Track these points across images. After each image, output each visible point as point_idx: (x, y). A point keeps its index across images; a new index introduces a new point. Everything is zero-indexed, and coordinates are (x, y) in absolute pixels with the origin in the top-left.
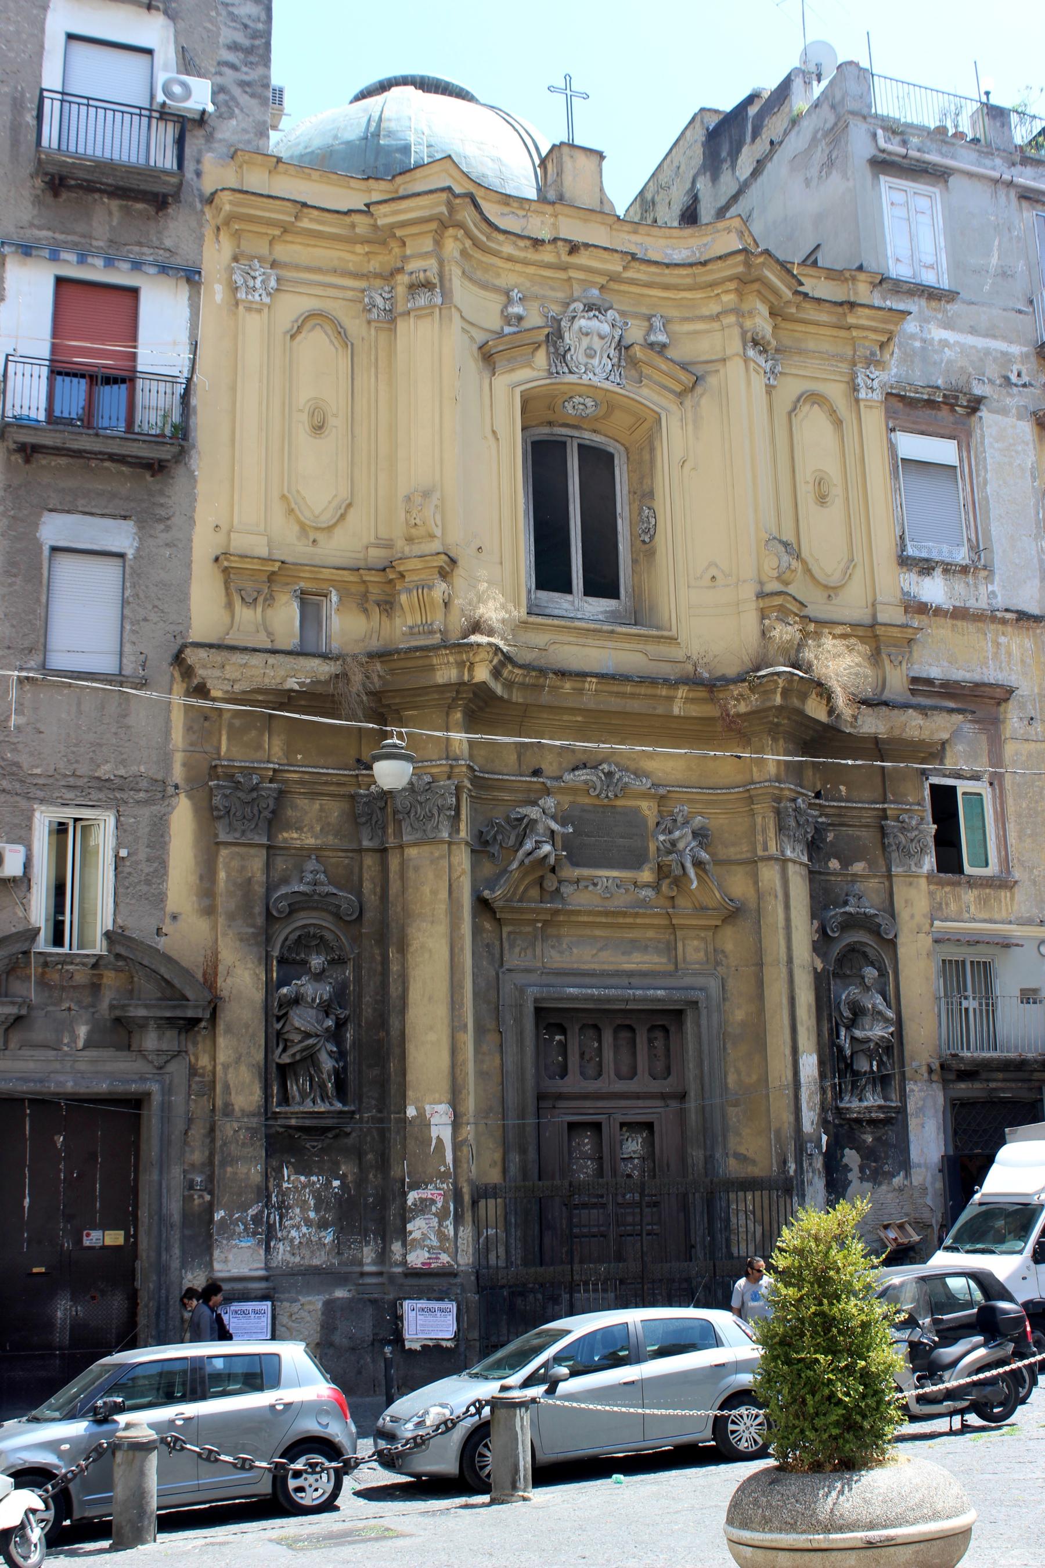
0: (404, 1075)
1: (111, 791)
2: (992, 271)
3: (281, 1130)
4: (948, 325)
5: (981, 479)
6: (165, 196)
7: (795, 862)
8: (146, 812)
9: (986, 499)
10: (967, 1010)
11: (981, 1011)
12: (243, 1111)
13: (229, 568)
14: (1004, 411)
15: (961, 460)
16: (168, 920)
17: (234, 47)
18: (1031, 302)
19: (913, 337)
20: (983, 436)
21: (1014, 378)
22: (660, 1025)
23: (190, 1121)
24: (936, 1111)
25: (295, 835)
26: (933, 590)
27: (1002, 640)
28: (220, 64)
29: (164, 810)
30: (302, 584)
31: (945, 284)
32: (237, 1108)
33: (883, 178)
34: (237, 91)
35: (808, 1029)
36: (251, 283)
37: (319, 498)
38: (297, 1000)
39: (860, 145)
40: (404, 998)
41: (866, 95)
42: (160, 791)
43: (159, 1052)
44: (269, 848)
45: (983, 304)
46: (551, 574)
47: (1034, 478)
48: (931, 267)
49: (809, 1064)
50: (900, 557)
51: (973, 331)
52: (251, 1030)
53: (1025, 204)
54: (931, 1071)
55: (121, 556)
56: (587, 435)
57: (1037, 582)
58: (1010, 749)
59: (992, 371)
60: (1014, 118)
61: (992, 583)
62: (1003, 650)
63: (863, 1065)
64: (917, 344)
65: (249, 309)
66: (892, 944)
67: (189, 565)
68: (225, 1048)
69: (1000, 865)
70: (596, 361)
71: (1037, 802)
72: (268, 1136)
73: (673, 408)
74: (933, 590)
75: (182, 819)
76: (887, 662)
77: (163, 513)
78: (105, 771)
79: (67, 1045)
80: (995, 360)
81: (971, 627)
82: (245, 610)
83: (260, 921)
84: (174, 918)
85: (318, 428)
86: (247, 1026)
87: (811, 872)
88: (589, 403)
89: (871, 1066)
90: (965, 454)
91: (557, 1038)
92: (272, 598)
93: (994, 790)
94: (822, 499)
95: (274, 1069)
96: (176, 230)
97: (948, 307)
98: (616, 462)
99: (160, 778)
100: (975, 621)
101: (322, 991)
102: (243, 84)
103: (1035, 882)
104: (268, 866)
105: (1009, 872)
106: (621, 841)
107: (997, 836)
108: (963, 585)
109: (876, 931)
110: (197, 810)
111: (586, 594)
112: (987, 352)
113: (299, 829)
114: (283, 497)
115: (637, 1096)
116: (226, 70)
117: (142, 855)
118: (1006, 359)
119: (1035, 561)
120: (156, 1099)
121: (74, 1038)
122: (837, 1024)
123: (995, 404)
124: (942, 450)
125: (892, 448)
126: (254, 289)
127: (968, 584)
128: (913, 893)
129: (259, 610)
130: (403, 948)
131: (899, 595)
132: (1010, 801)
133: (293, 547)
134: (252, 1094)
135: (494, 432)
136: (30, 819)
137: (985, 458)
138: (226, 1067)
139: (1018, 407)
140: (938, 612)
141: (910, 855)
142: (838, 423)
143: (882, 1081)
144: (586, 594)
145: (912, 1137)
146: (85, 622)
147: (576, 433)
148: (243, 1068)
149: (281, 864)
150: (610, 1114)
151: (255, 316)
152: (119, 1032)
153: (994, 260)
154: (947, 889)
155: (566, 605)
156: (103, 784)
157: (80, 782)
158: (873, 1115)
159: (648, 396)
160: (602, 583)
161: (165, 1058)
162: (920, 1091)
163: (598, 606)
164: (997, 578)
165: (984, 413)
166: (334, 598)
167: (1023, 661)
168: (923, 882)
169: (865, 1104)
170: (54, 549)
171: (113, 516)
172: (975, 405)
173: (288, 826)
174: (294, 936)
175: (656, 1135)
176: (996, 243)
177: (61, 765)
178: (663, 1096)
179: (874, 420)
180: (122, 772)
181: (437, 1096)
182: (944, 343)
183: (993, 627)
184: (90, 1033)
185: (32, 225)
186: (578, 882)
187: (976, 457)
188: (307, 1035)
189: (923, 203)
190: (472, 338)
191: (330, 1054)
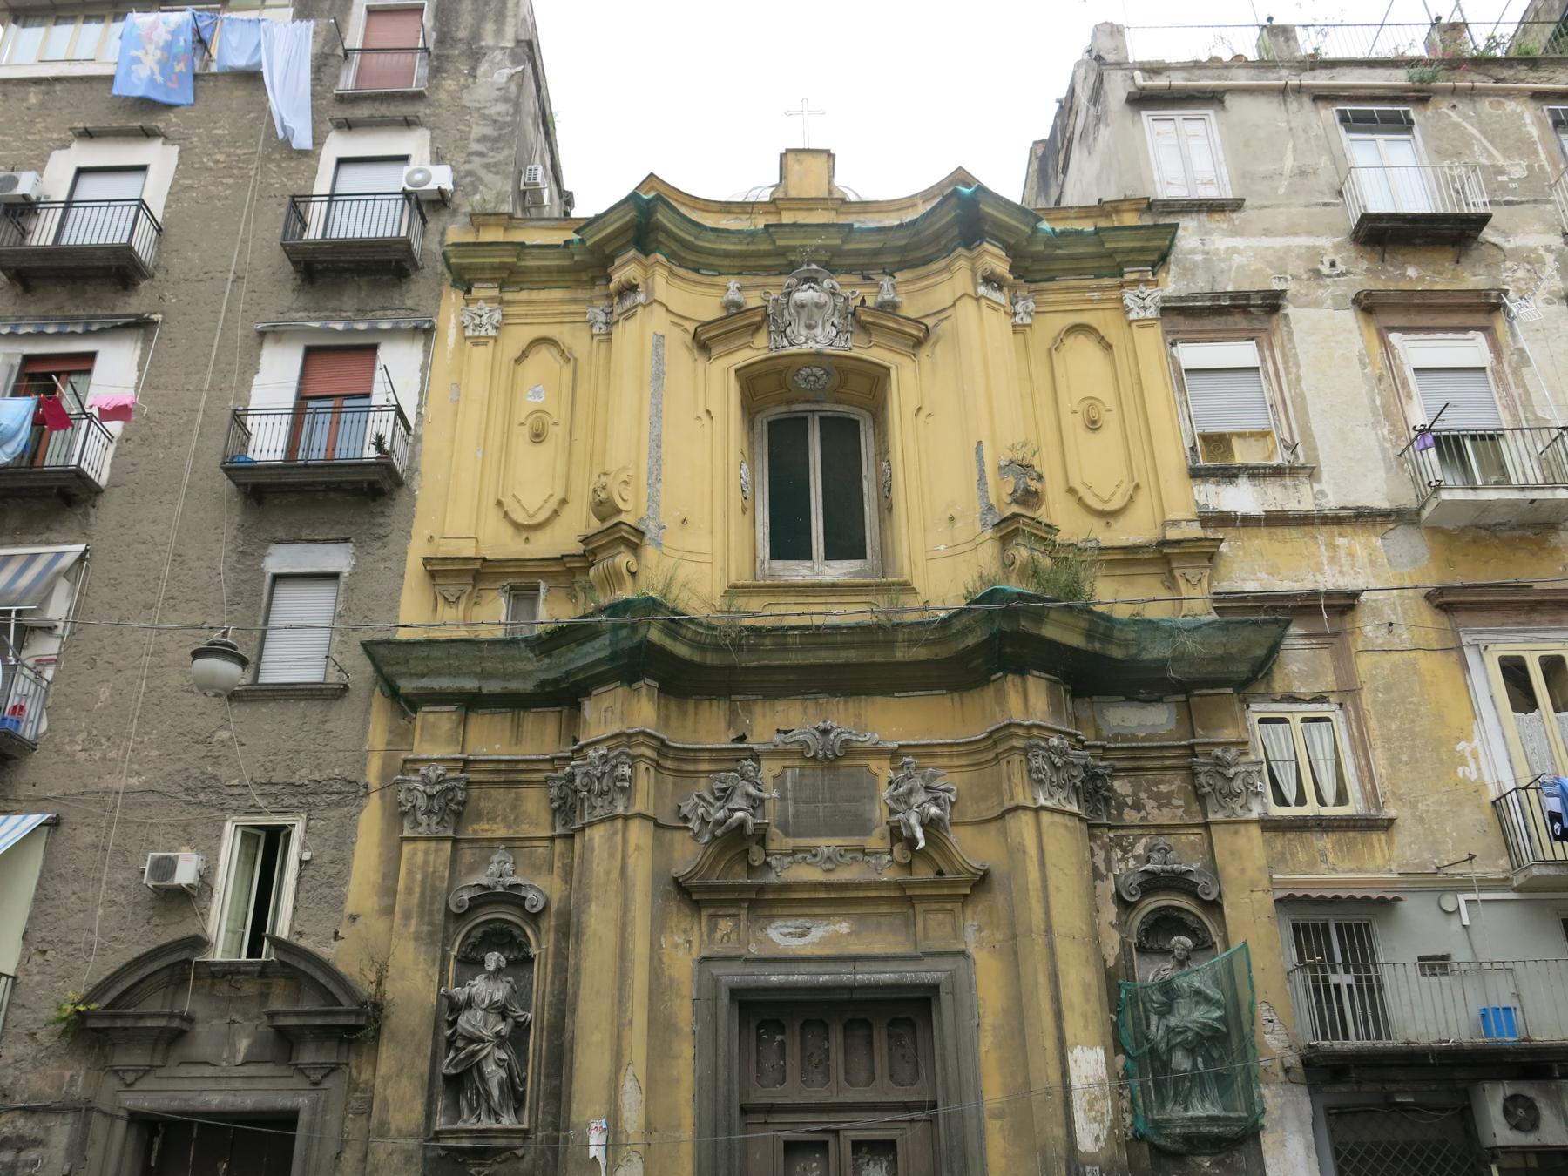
1: (304, 794)
2: (1287, 172)
3: (442, 1153)
4: (1236, 232)
5: (1293, 377)
6: (398, 262)
7: (1052, 810)
8: (334, 814)
9: (1302, 396)
10: (1337, 987)
11: (1360, 989)
12: (399, 1131)
13: (440, 571)
14: (1317, 304)
15: (1263, 360)
16: (345, 922)
17: (480, 140)
18: (1340, 193)
19: (1193, 252)
20: (1290, 333)
21: (1325, 269)
22: (903, 1016)
23: (343, 1144)
24: (1302, 1123)
25: (486, 827)
26: (1241, 498)
27: (1340, 541)
28: (469, 154)
29: (354, 811)
30: (510, 580)
31: (1228, 193)
32: (393, 1127)
33: (1144, 113)
34: (483, 173)
35: (1084, 1015)
36: (477, 320)
37: (532, 499)
38: (469, 1003)
39: (1117, 89)
40: (576, 994)
41: (1121, 48)
42: (354, 790)
43: (316, 1066)
44: (455, 841)
45: (1278, 206)
46: (788, 539)
47: (1364, 365)
48: (1211, 182)
49: (1089, 1063)
50: (1191, 469)
51: (1267, 232)
53: (1320, 104)
54: (1287, 1071)
55: (334, 576)
56: (827, 407)
57: (1382, 474)
58: (1364, 664)
59: (1296, 267)
60: (1299, 32)
61: (1319, 481)
62: (1342, 553)
63: (1181, 1061)
64: (1199, 257)
65: (476, 344)
66: (1215, 907)
67: (402, 576)
68: (388, 1055)
69: (1366, 800)
70: (819, 331)
71: (1413, 721)
72: (425, 1158)
73: (907, 361)
74: (1241, 498)
75: (371, 819)
76: (1182, 582)
77: (381, 531)
78: (301, 776)
79: (226, 1060)
80: (1299, 257)
81: (1294, 533)
82: (448, 609)
83: (439, 918)
84: (354, 918)
85: (538, 437)
86: (413, 1033)
87: (1090, 826)
88: (819, 372)
89: (1195, 1063)
90: (1267, 354)
91: (779, 1038)
92: (479, 596)
93: (1346, 712)
94: (1093, 425)
95: (440, 1081)
96: (415, 293)
97: (1235, 215)
98: (862, 427)
99: (351, 778)
100: (1299, 525)
101: (500, 992)
102: (487, 166)
103: (1421, 820)
104: (454, 860)
105: (1379, 809)
106: (846, 806)
107: (1358, 767)
108: (1278, 489)
109: (1189, 889)
110: (384, 808)
111: (827, 558)
112: (1288, 249)
113: (492, 820)
114: (499, 503)
115: (874, 1107)
116: (477, 159)
117: (326, 858)
118: (1315, 253)
119: (1377, 452)
120: (303, 1118)
121: (233, 1054)
122: (1146, 1011)
123: (1303, 299)
124: (1242, 353)
125: (1175, 362)
126: (481, 325)
127: (1285, 486)
128: (1241, 842)
129: (462, 607)
130: (579, 936)
131: (1194, 509)
132: (1373, 723)
133: (500, 543)
135: (708, 412)
136: (221, 828)
137: (1295, 355)
138: (386, 1080)
139: (1334, 298)
140: (1247, 521)
141: (1234, 795)
142: (1108, 347)
143: (1223, 1082)
144: (827, 558)
145: (1268, 1160)
146: (301, 643)
147: (816, 407)
148: (405, 1082)
149: (467, 856)
150: (837, 1132)
151: (481, 348)
152: (283, 1043)
153: (1289, 163)
154: (1290, 835)
155: (804, 572)
156: (295, 788)
157: (274, 790)
158: (1204, 1130)
159: (877, 355)
160: (846, 542)
161: (323, 1072)
162: (1274, 1096)
163: (839, 571)
164: (1325, 476)
165: (1290, 310)
166: (542, 589)
167: (1372, 563)
168: (1255, 831)
169: (1190, 1113)
170: (277, 578)
171: (336, 541)
172: (1272, 303)
173: (479, 817)
174: (478, 932)
175: (899, 1157)
176: (1290, 146)
177: (257, 775)
178: (907, 1107)
179: (1150, 340)
180: (316, 776)
182: (1234, 251)
183: (1323, 529)
184: (251, 1046)
185: (290, 309)
186: (794, 852)
187: (1284, 355)
188: (471, 1040)
189: (1196, 127)
190: (686, 330)
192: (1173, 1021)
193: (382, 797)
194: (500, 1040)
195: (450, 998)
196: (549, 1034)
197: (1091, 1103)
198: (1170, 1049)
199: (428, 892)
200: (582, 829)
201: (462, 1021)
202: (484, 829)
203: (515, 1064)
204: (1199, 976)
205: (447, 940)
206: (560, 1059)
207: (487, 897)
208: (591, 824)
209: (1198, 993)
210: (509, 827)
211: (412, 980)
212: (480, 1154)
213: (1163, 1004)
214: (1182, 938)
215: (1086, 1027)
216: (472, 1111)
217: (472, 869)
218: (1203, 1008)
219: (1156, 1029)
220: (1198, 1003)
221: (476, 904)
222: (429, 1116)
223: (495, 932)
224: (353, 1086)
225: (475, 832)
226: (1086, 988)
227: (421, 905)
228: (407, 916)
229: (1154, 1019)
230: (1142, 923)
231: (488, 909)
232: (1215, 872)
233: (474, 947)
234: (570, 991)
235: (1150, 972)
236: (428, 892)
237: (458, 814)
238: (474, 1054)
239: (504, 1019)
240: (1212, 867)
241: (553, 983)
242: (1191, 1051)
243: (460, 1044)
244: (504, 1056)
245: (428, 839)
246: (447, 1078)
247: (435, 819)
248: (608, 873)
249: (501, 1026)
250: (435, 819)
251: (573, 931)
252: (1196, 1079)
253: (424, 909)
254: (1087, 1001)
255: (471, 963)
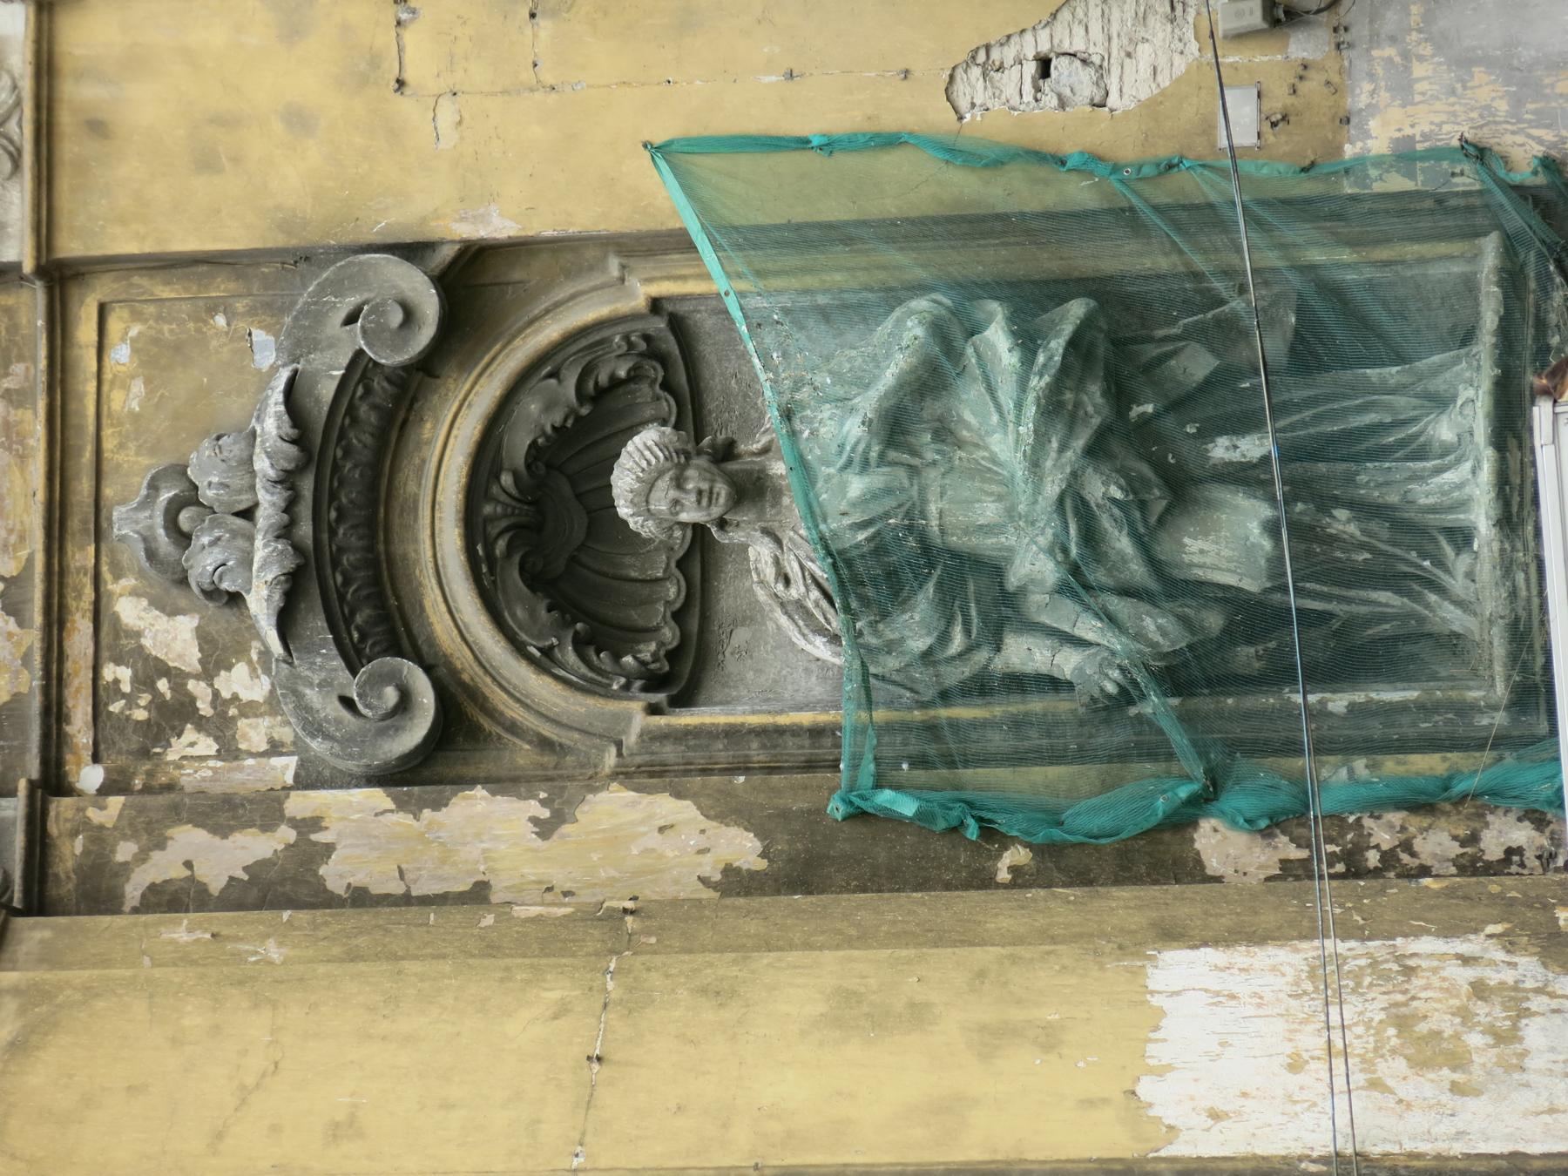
35: (992, 1040)
63: (1231, 543)
66: (475, 284)
122: (981, 687)
162: (1403, 89)
192: (1034, 565)
197: (1431, 1052)
198: (1172, 586)
204: (816, 396)
209: (894, 428)
213: (948, 604)
214: (624, 480)
215: (1049, 1039)
218: (969, 406)
219: (1074, 650)
220: (944, 432)
226: (852, 1015)
229: (1023, 653)
230: (545, 662)
232: (304, 258)
235: (790, 657)
240: (281, 271)
242: (1179, 489)
252: (1309, 479)
254: (919, 1015)
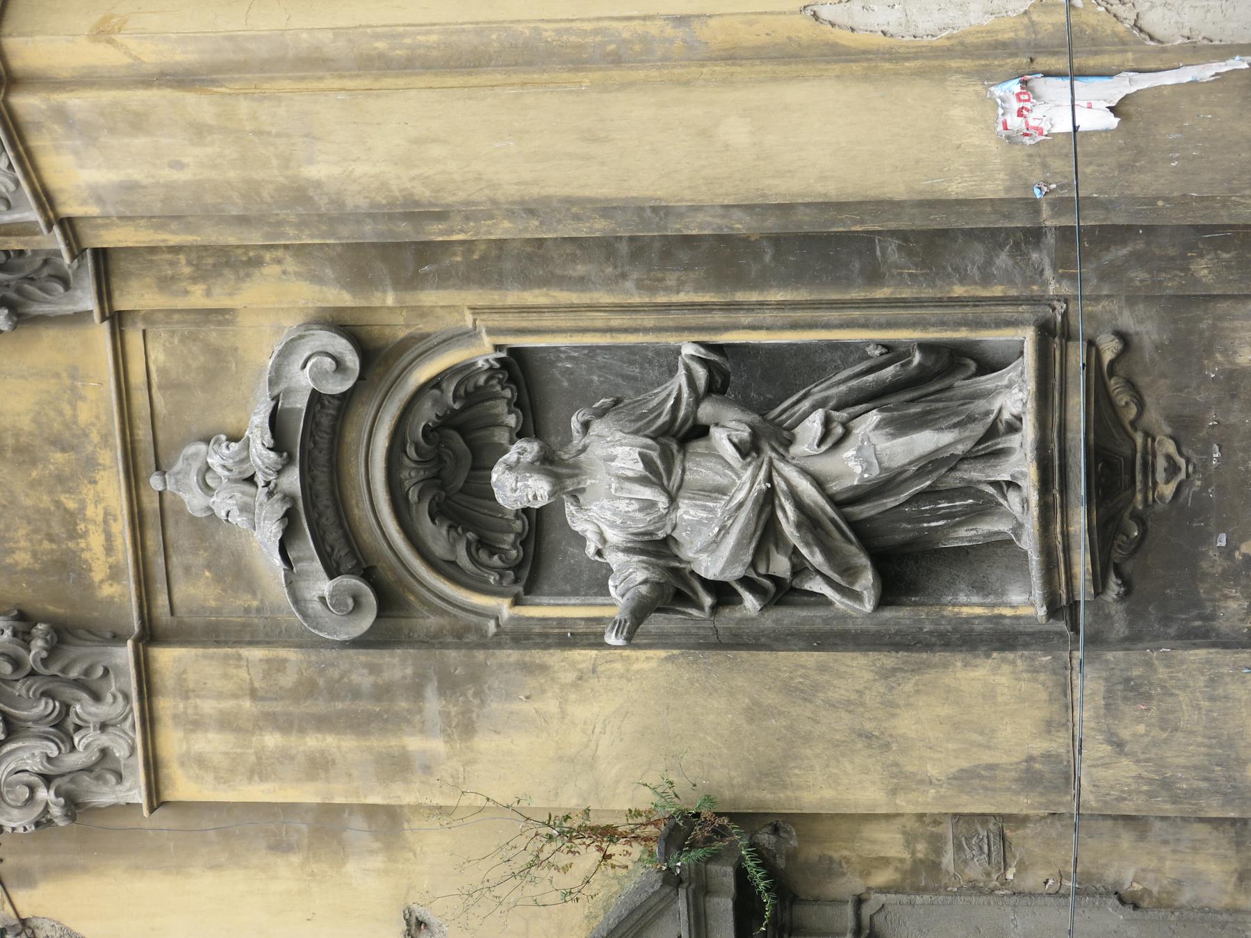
0: (892, 204)
3: (1114, 587)
12: (1049, 727)
23: (1089, 889)
25: (96, 540)
32: (1040, 746)
38: (657, 548)
40: (606, 209)
44: (151, 635)
52: (771, 699)
72: (1132, 640)
83: (396, 665)
86: (756, 712)
101: (613, 454)
110: (65, 870)
113: (71, 522)
130: (418, 213)
134: (989, 695)
138: (899, 781)
148: (904, 725)
149: (195, 591)
173: (67, 566)
174: (436, 536)
181: (957, 112)
188: (766, 533)
191: (833, 439)
193: (27, 879)
194: (766, 439)
195: (641, 611)
196: (741, 281)
199: (320, 706)
200: (68, 226)
201: (711, 566)
202: (105, 550)
203: (835, 387)
205: (468, 634)
206: (820, 245)
207: (321, 520)
208: (45, 199)
210: (91, 464)
211: (600, 728)
212: (1113, 471)
216: (985, 507)
217: (237, 573)
221: (345, 551)
222: (1004, 638)
223: (436, 480)
224: (922, 877)
225: (115, 574)
227: (358, 724)
228: (398, 766)
231: (360, 511)
233: (484, 545)
234: (599, 227)
236: (320, 706)
237: (63, 634)
238: (809, 520)
239: (701, 431)
241: (582, 283)
243: (781, 565)
244: (814, 425)
245: (149, 722)
246: (889, 595)
247: (83, 708)
248: (199, 131)
249: (721, 439)
250: (83, 708)
251: (405, 231)
253: (372, 714)
255: (533, 552)
